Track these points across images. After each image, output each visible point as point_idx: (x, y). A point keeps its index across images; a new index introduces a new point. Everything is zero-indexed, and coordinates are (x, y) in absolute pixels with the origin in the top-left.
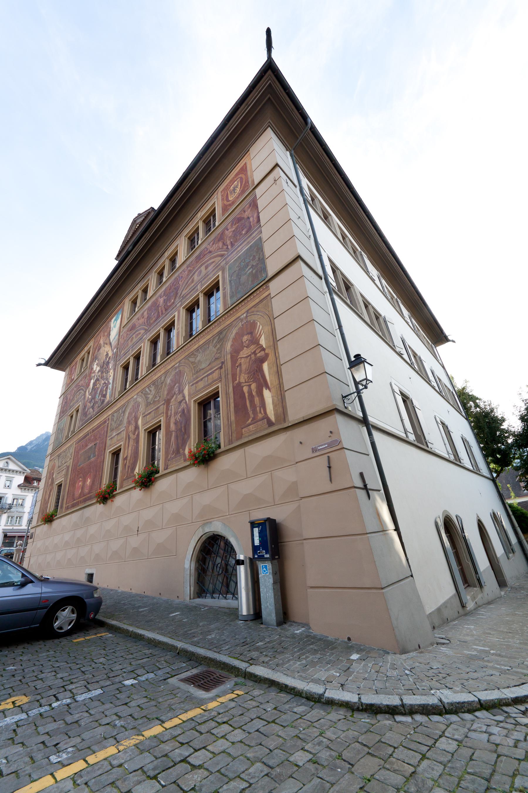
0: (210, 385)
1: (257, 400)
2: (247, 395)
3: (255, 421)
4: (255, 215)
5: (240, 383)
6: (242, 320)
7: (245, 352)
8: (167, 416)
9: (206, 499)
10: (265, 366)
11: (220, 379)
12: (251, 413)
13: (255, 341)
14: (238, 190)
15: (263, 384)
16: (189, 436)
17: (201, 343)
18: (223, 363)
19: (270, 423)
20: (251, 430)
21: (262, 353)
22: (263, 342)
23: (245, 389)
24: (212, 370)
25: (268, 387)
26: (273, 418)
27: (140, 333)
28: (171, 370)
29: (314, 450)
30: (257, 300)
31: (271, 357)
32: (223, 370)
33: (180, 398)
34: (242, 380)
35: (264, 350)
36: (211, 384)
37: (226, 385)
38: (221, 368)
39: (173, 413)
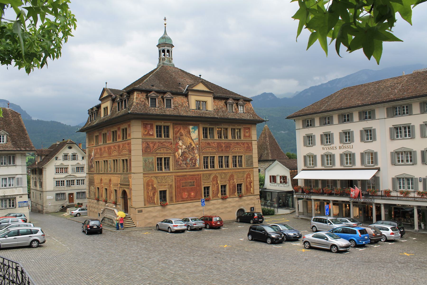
7: (248, 179)
9: (240, 203)
13: (250, 178)
15: (251, 187)
33: (233, 181)
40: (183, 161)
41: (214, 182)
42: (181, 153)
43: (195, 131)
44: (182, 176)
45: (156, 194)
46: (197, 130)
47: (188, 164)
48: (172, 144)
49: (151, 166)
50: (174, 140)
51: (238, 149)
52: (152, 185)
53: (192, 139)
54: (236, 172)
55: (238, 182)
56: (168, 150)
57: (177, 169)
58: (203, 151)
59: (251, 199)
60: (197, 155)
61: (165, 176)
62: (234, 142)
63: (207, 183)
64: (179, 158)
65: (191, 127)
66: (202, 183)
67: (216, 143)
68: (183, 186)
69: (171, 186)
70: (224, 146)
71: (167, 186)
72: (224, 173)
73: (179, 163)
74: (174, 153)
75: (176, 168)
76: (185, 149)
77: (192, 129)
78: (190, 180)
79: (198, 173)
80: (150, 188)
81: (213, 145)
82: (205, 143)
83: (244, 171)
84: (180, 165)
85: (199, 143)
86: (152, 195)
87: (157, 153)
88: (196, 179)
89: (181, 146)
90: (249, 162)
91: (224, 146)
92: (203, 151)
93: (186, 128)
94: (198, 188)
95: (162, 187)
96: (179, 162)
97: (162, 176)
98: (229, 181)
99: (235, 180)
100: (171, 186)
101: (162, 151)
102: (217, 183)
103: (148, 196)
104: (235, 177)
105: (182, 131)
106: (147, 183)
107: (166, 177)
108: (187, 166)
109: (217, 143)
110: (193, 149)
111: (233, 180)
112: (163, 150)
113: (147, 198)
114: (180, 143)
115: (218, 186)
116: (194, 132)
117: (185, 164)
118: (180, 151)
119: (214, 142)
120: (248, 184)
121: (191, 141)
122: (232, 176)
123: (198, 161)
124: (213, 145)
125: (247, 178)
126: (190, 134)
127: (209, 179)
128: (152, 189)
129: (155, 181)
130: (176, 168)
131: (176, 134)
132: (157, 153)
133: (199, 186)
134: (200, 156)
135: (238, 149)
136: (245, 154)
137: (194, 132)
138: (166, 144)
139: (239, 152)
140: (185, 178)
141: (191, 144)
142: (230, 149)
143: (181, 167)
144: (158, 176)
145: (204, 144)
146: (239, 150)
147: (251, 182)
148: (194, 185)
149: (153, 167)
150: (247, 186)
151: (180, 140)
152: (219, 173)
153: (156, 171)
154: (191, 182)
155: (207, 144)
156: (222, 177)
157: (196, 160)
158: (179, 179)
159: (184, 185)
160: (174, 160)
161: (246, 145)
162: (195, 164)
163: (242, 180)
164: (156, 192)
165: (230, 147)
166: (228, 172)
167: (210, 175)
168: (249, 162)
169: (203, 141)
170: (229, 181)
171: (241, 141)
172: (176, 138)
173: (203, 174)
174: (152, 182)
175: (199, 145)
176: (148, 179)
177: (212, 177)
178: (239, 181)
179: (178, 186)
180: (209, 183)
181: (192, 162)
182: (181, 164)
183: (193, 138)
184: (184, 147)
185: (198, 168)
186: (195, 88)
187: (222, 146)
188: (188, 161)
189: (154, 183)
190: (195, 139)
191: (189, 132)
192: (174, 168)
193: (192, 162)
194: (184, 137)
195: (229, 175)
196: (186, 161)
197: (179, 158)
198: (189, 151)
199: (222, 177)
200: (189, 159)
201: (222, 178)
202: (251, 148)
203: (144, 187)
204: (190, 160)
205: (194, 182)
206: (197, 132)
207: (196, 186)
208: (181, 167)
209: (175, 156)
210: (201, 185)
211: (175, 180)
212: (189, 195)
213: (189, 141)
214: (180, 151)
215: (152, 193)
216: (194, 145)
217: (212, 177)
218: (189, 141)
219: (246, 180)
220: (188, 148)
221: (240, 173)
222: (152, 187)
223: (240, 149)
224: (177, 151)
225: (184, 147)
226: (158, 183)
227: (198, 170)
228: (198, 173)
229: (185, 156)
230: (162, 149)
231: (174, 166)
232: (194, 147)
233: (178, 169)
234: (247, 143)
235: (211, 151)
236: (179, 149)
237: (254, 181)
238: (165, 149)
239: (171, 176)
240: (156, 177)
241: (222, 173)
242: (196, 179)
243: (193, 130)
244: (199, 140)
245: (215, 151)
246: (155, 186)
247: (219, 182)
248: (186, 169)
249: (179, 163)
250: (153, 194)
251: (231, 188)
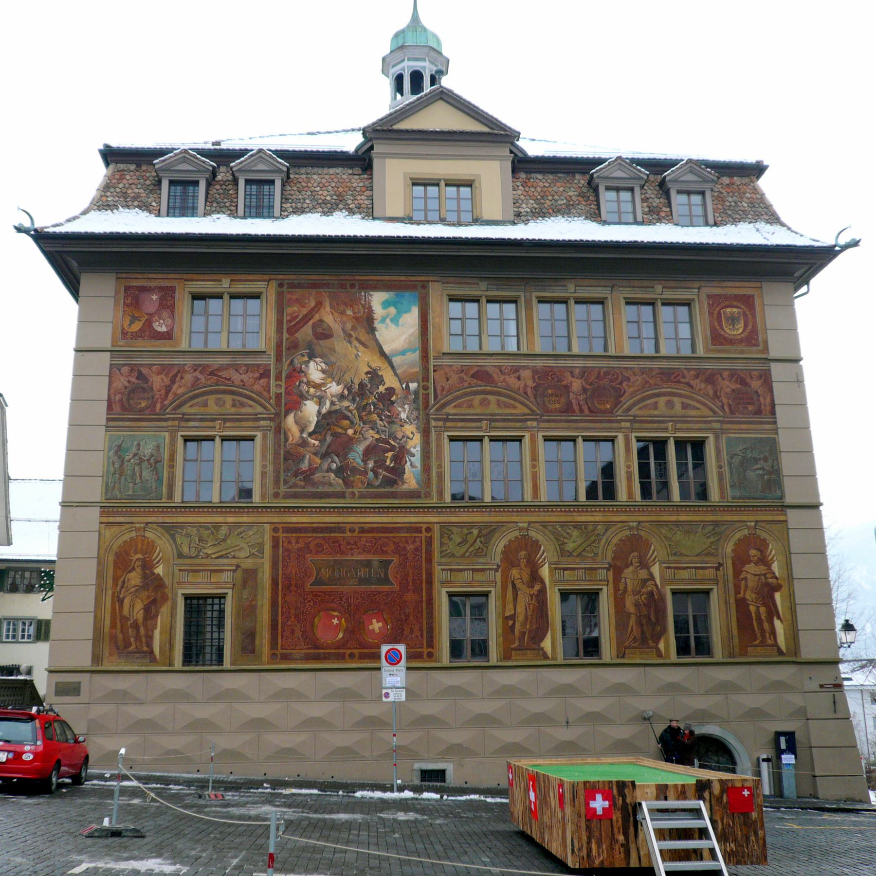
0: (702, 581)
1: (766, 625)
2: (754, 615)
3: (763, 644)
4: (768, 400)
5: (744, 600)
6: (749, 528)
7: (751, 568)
8: (616, 589)
10: (778, 596)
11: (716, 581)
12: (758, 635)
13: (764, 561)
14: (740, 331)
15: (773, 612)
16: (664, 631)
17: (683, 518)
18: (720, 565)
19: (780, 652)
20: (756, 653)
21: (774, 581)
22: (775, 567)
23: (752, 609)
24: (703, 565)
25: (779, 618)
26: (784, 650)
27: (515, 407)
28: (620, 525)
29: (821, 686)
30: (769, 518)
31: (785, 588)
32: (720, 573)
33: (643, 574)
34: (748, 597)
35: (776, 578)
36: (702, 580)
37: (725, 592)
38: (717, 569)
39: (630, 588)
40: (324, 456)
41: (515, 573)
42: (314, 420)
43: (400, 313)
44: (315, 530)
45: (165, 610)
46: (415, 311)
47: (354, 470)
48: (265, 374)
49: (146, 474)
50: (279, 359)
51: (670, 405)
52: (147, 566)
53: (382, 354)
54: (660, 524)
55: (673, 581)
56: (242, 405)
57: (287, 496)
58: (450, 410)
59: (779, 686)
60: (409, 429)
61: (217, 527)
62: (643, 371)
63: (468, 575)
64: (304, 443)
65: (377, 299)
66: (439, 573)
67: (526, 374)
68: (318, 582)
69: (250, 576)
70: (577, 385)
71: (226, 577)
72: (577, 526)
73: (305, 466)
74: (278, 419)
75: (283, 489)
76: (342, 397)
77: (386, 304)
78: (365, 550)
79: (412, 518)
80: (135, 578)
81: (512, 380)
82: (462, 370)
83: (716, 524)
84: (308, 476)
85: (426, 369)
86: (138, 614)
87: (185, 418)
88: (399, 550)
89: (317, 386)
90: (752, 475)
91: (577, 385)
92: (450, 410)
93: (352, 302)
94: (410, 597)
95: (200, 578)
96: (300, 458)
97: (200, 526)
98: (617, 570)
99: (656, 570)
100: (250, 576)
101: (213, 408)
102: (535, 577)
103: (119, 619)
104: (657, 550)
105: (328, 317)
106: (118, 555)
107: (224, 531)
108: (347, 483)
109: (535, 371)
110: (388, 397)
111: (644, 565)
112: (220, 403)
113: (113, 626)
114: (315, 372)
115: (541, 598)
116: (395, 320)
117: (339, 472)
118: (310, 409)
119: (516, 369)
120: (750, 596)
121: (377, 363)
122: (633, 548)
123: (417, 460)
124: (512, 380)
125: (740, 561)
126: (372, 330)
127: (480, 553)
128: (144, 587)
129: (163, 545)
130: (283, 489)
131: (292, 331)
132: (185, 418)
133: (418, 590)
134: (426, 433)
135: (670, 405)
136: (724, 431)
137: (395, 320)
138: (236, 377)
139: (677, 420)
140: (336, 541)
141: (375, 376)
142: (617, 403)
143: (314, 484)
144: (182, 525)
145: (454, 378)
146: (678, 407)
147: (778, 588)
148: (386, 581)
149: (159, 480)
150: (742, 605)
151: (312, 356)
152: (544, 524)
153: (170, 496)
154: (368, 564)
155: (473, 376)
156: (570, 546)
157: (401, 455)
158: (295, 546)
159: (326, 574)
160: (276, 454)
161: (727, 386)
162: (398, 472)
163: (710, 573)
164: (165, 598)
165: (619, 394)
166: (609, 525)
167: (488, 533)
168: (752, 475)
169: (446, 362)
170: (617, 570)
171: (694, 365)
172: (294, 346)
173: (445, 528)
174: (150, 547)
175: (426, 379)
176: (126, 537)
177: (499, 545)
178: (685, 574)
179: (287, 578)
180: (478, 577)
181: (380, 464)
182: (312, 470)
183: (387, 349)
184: (334, 388)
185: (413, 494)
186: (395, 127)
187: (567, 388)
188: (356, 456)
189: (157, 554)
190: (403, 353)
191: (368, 322)
192: (271, 490)
193: (380, 464)
194: (340, 345)
195: (616, 536)
196: (343, 456)
197: (304, 443)
198: (362, 408)
199: (570, 546)
200: (360, 448)
201: (563, 553)
202: (765, 401)
203: (100, 574)
204: (368, 453)
205: (385, 564)
206: (412, 318)
207: (396, 587)
208: (314, 484)
209: (280, 430)
210: (430, 582)
211: (275, 545)
212: (356, 630)
213: (366, 360)
214: (310, 409)
215: (139, 606)
216: (390, 381)
217: (499, 545)
218: (366, 360)
219: (737, 572)
220: (358, 392)
221: (687, 533)
222: (145, 577)
223: (685, 406)
224: (294, 403)
225: (334, 388)
226: (180, 555)
227: (415, 502)
228: (412, 518)
229: (335, 435)
230: (212, 399)
231: (270, 481)
232: (391, 391)
233: (295, 496)
234: (733, 374)
235: (493, 409)
236: (303, 397)
237: (790, 578)
238: (228, 398)
239: (251, 525)
240: (171, 530)
241: (563, 524)
242: (399, 550)
243: (392, 310)
244: (425, 356)
245: (521, 409)
246: (159, 570)
247: (545, 572)
248: (342, 495)
249: (305, 466)
250: (147, 610)
251: (630, 607)
